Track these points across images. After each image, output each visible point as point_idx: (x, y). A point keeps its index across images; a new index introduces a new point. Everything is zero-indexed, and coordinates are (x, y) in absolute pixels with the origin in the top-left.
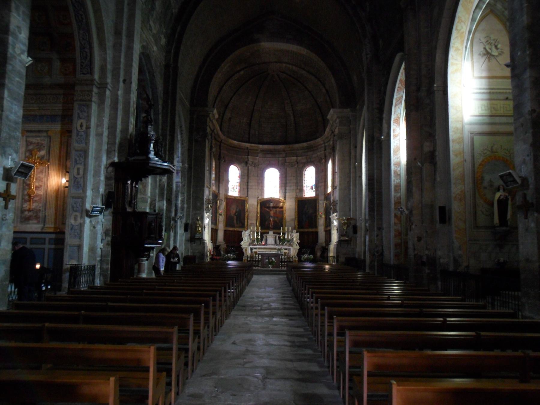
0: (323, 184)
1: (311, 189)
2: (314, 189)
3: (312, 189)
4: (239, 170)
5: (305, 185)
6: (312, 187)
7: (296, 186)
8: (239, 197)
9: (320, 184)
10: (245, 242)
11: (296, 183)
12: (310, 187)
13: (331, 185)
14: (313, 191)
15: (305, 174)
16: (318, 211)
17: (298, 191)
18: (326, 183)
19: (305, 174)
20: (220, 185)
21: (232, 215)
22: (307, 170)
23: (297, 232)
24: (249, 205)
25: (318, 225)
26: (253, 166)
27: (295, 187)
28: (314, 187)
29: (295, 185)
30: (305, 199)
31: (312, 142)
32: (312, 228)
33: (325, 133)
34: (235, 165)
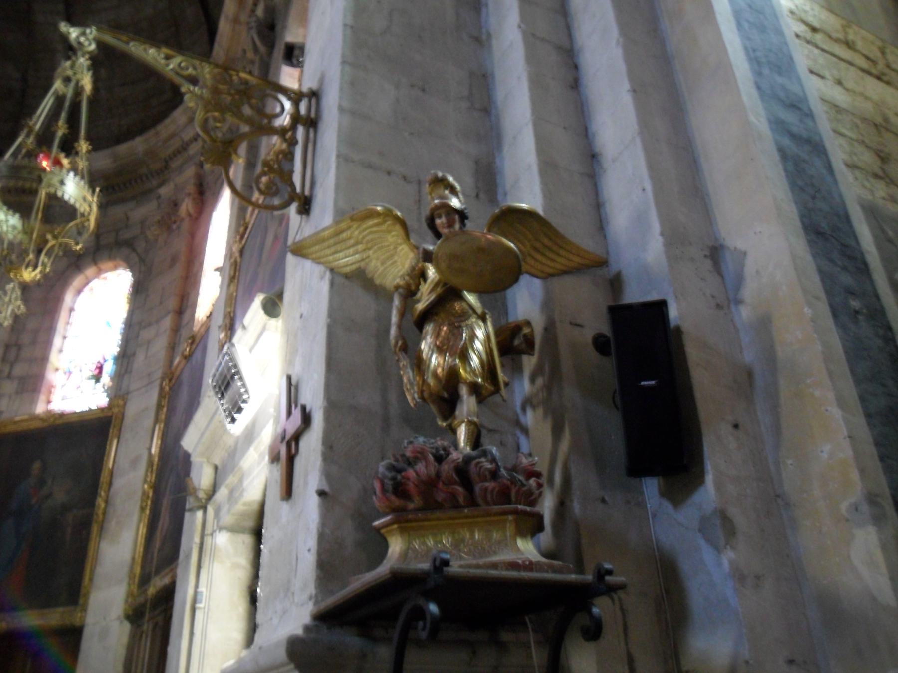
0: (167, 322)
2: (106, 379)
3: (97, 378)
5: (55, 358)
9: (146, 334)
12: (91, 370)
13: (220, 263)
14: (100, 385)
15: (76, 306)
16: (110, 484)
18: (186, 316)
19: (72, 310)
22: (87, 289)
25: (91, 580)
28: (109, 368)
30: (36, 424)
31: (138, 145)
32: (46, 602)
33: (224, 27)
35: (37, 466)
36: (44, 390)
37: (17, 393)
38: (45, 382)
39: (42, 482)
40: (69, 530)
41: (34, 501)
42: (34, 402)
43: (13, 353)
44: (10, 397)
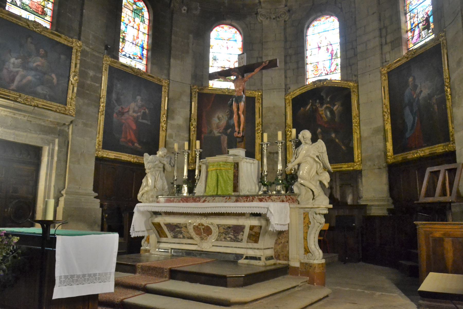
1: (424, 29)
4: (241, 34)
6: (427, 20)
7: (381, 37)
8: (234, 91)
10: (147, 192)
11: (380, 30)
17: (387, 48)
20: (172, 60)
21: (216, 133)
23: (314, 140)
24: (263, 108)
26: (274, 19)
27: (377, 39)
29: (377, 33)
34: (229, 21)
35: (411, 79)
36: (404, 44)
37: (392, 50)
38: (403, 39)
39: (415, 87)
40: (436, 107)
41: (415, 96)
42: (400, 51)
43: (384, 32)
44: (390, 52)
